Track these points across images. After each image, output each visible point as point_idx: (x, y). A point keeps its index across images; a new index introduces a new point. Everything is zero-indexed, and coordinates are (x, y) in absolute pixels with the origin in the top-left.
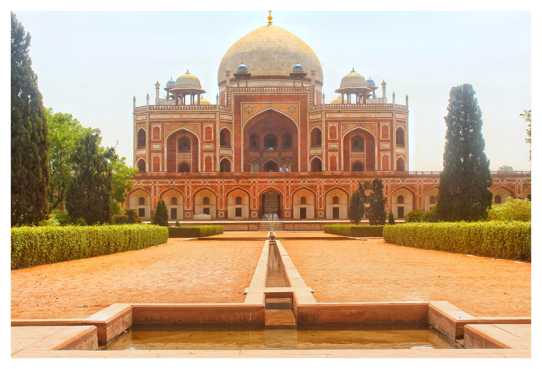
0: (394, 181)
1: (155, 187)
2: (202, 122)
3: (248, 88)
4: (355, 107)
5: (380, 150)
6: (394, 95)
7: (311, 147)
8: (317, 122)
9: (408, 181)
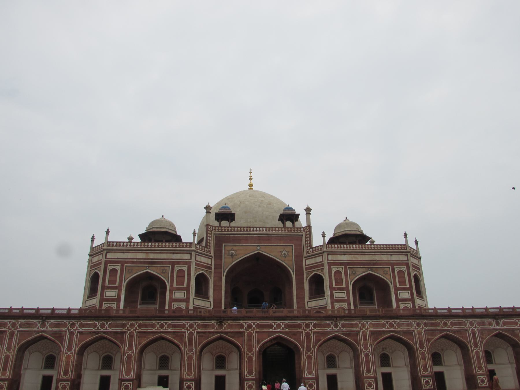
0: (483, 324)
1: (72, 334)
2: (173, 264)
3: (231, 227)
4: (362, 247)
5: (398, 301)
6: (406, 235)
7: (310, 298)
8: (317, 267)
9: (505, 324)
